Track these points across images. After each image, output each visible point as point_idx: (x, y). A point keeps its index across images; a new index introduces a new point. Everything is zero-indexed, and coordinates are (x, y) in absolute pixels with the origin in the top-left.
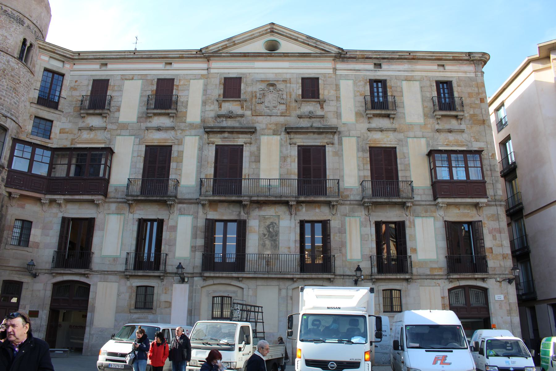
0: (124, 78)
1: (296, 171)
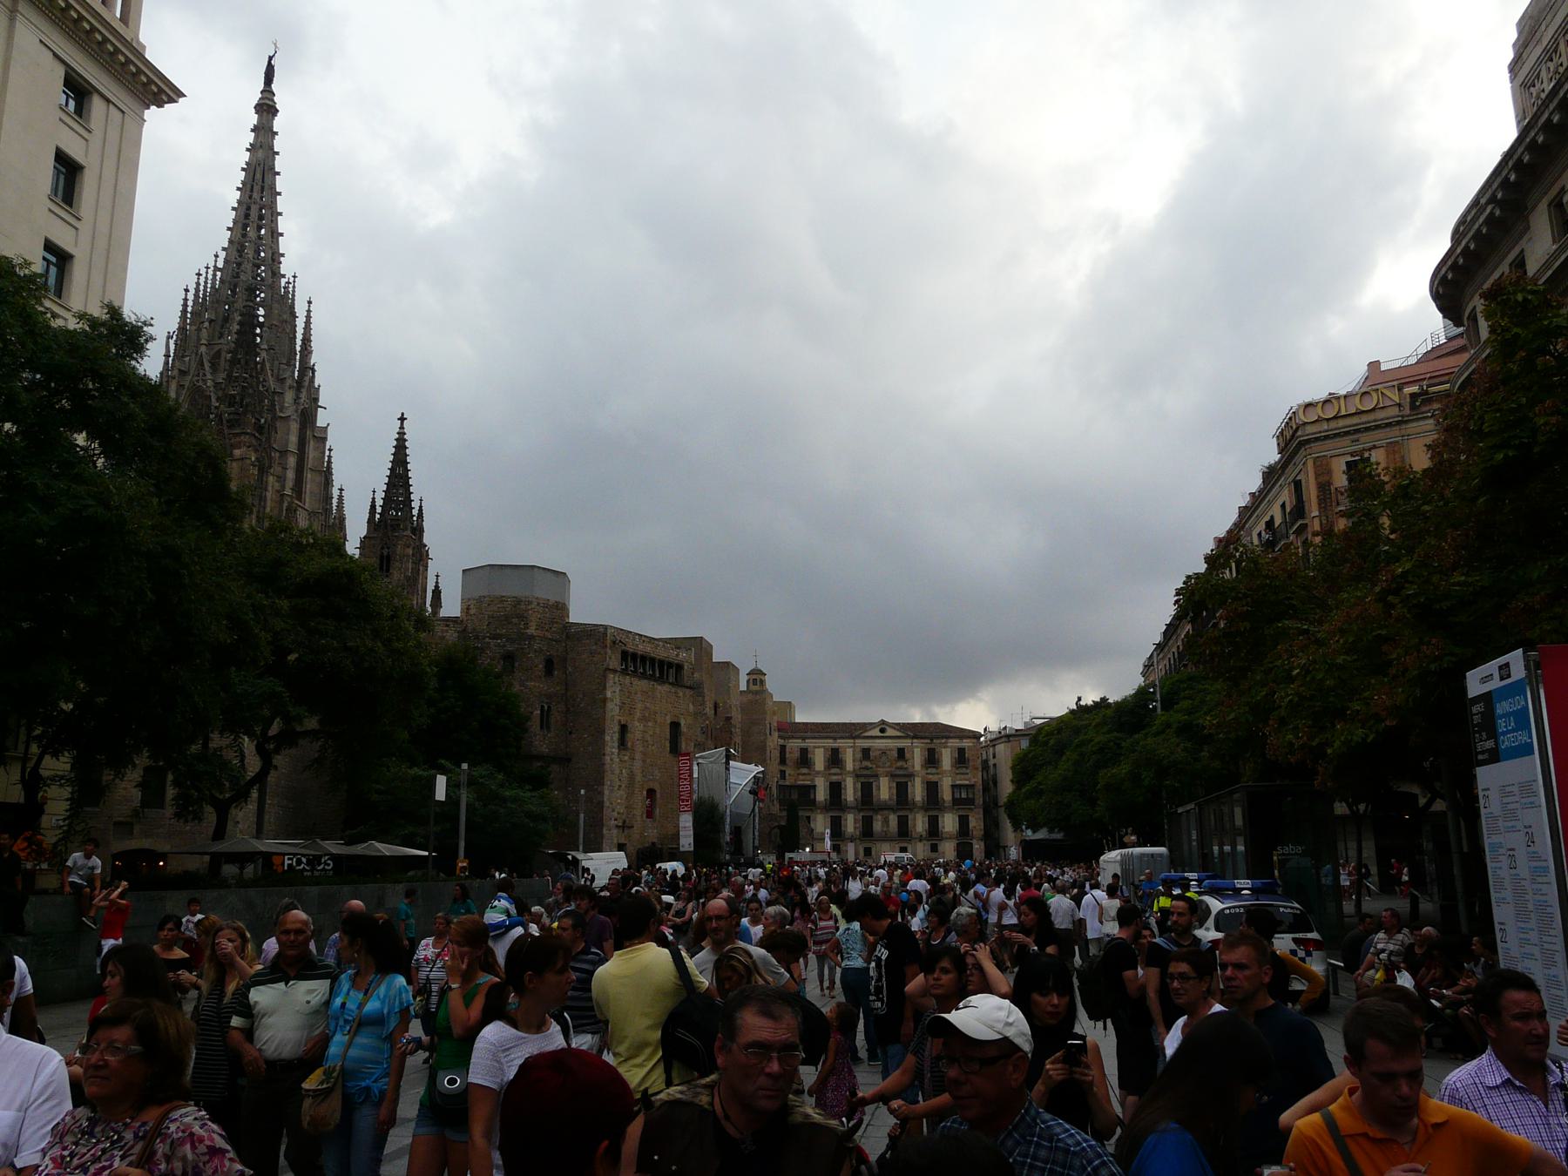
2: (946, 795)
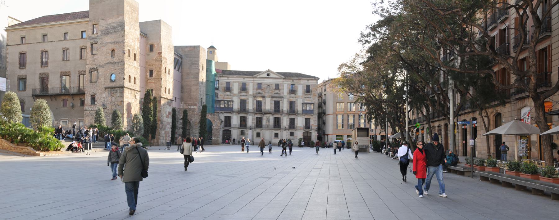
0: (234, 82)
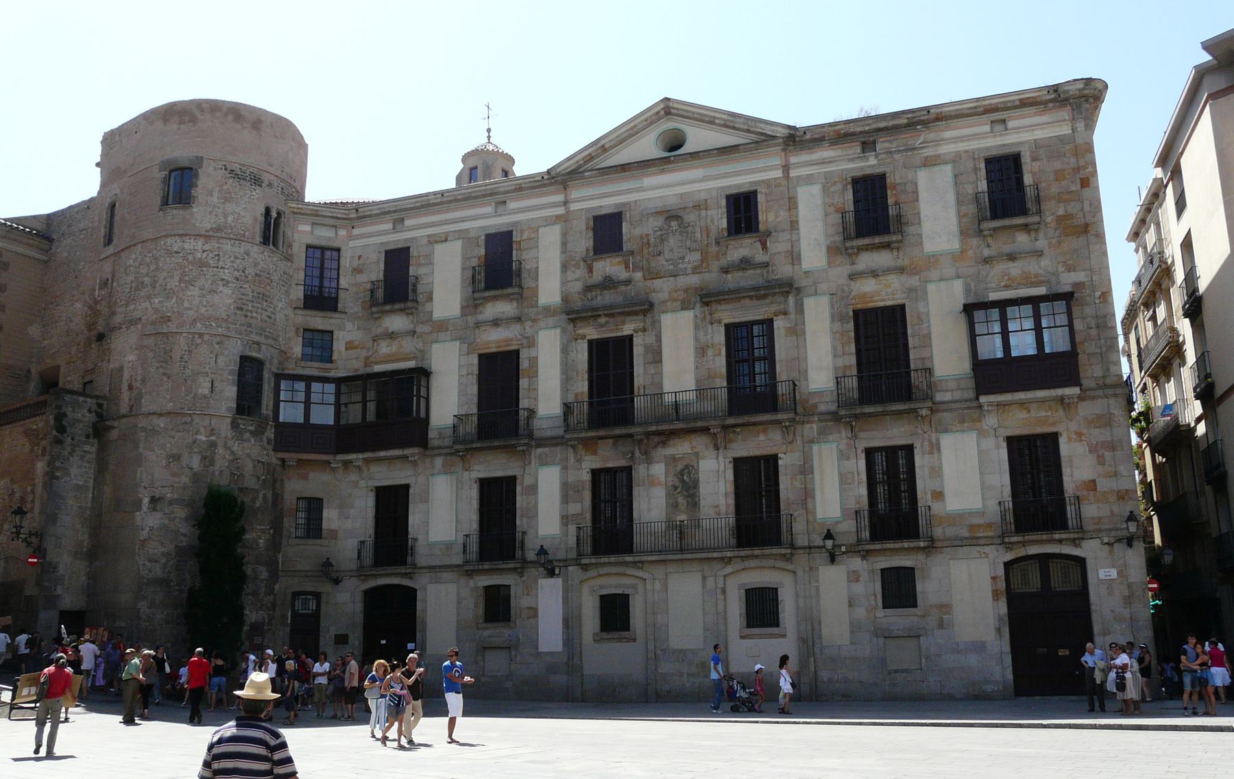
0: (433, 240)
1: (724, 371)
2: (943, 351)
